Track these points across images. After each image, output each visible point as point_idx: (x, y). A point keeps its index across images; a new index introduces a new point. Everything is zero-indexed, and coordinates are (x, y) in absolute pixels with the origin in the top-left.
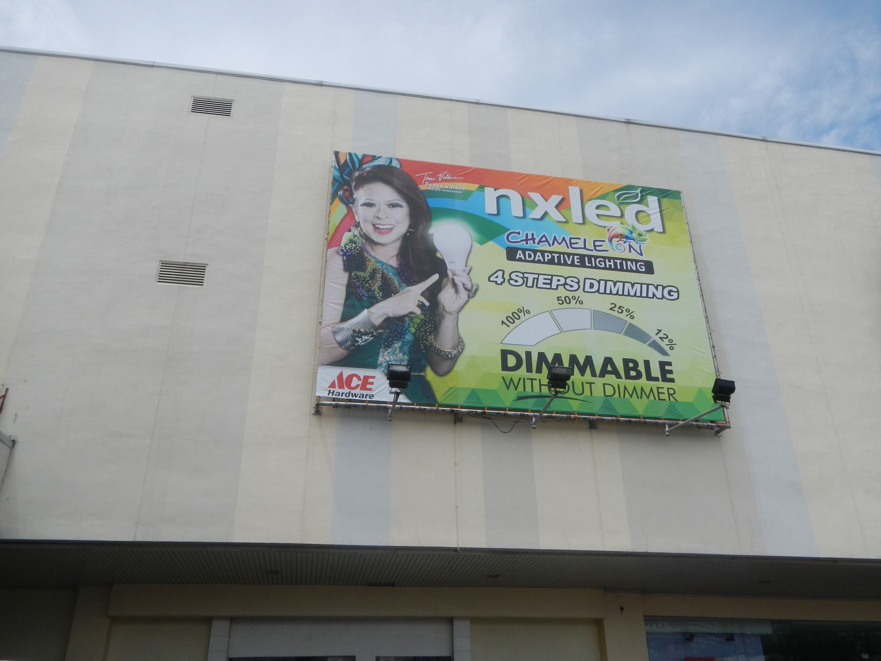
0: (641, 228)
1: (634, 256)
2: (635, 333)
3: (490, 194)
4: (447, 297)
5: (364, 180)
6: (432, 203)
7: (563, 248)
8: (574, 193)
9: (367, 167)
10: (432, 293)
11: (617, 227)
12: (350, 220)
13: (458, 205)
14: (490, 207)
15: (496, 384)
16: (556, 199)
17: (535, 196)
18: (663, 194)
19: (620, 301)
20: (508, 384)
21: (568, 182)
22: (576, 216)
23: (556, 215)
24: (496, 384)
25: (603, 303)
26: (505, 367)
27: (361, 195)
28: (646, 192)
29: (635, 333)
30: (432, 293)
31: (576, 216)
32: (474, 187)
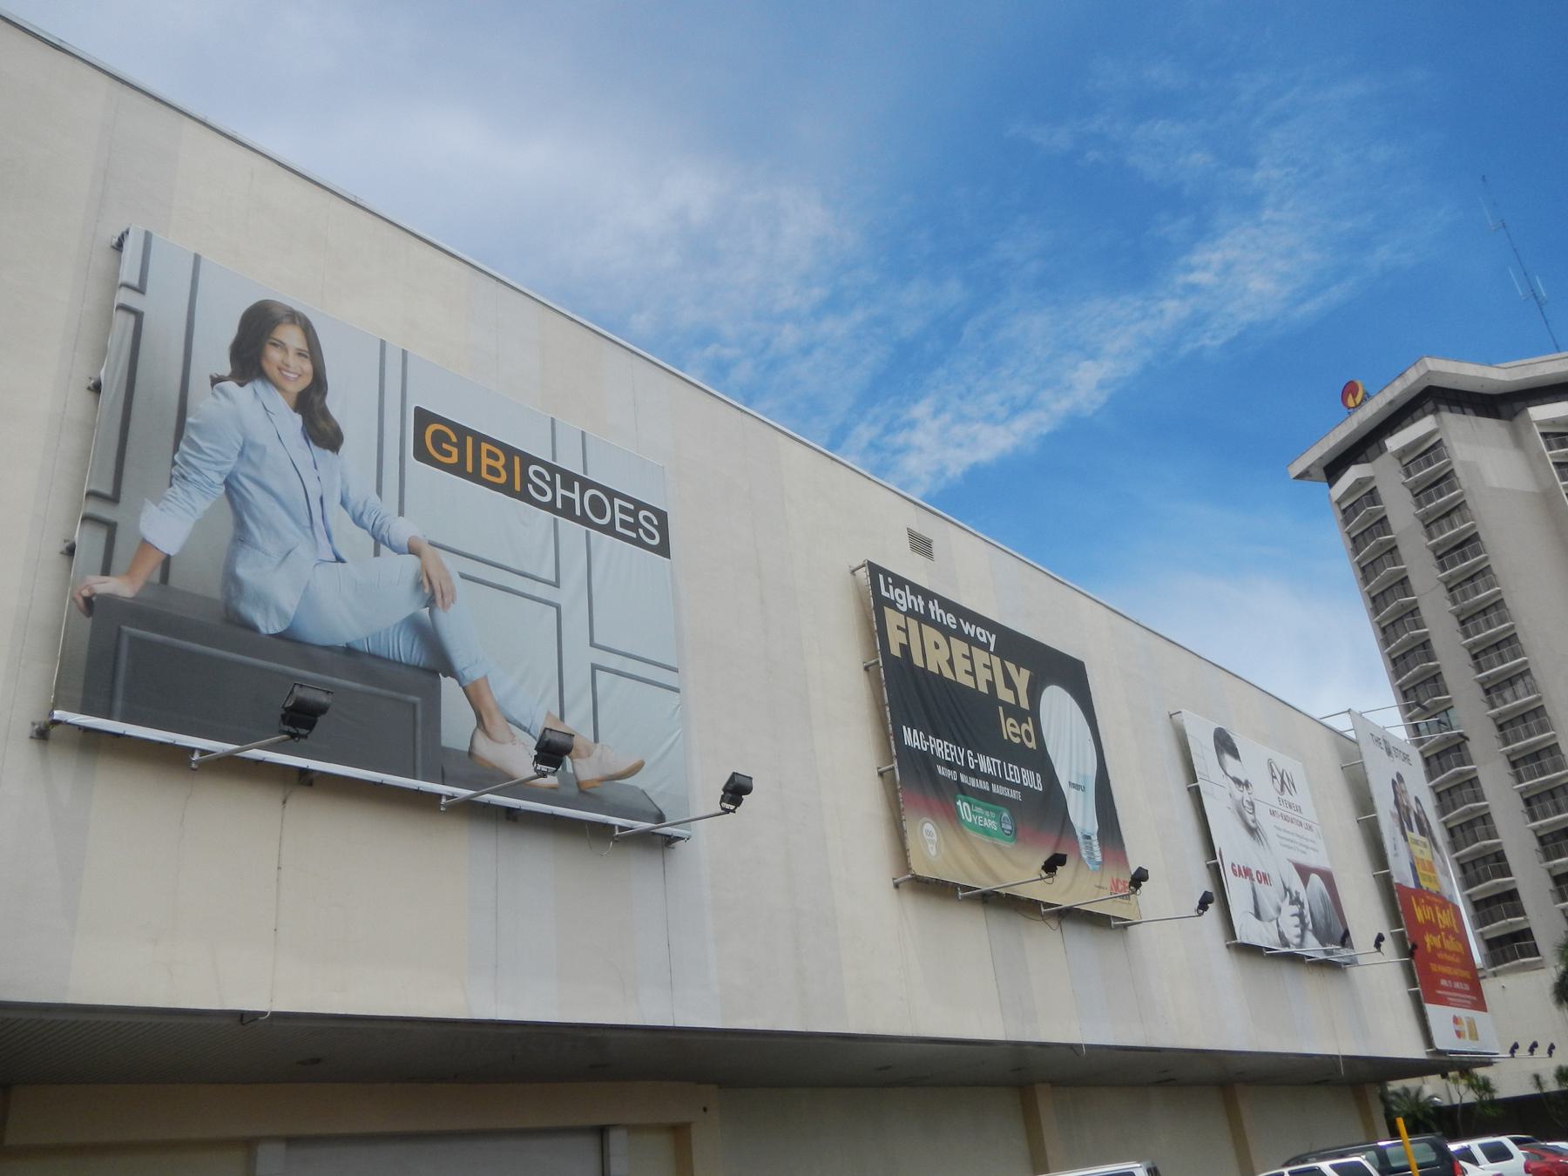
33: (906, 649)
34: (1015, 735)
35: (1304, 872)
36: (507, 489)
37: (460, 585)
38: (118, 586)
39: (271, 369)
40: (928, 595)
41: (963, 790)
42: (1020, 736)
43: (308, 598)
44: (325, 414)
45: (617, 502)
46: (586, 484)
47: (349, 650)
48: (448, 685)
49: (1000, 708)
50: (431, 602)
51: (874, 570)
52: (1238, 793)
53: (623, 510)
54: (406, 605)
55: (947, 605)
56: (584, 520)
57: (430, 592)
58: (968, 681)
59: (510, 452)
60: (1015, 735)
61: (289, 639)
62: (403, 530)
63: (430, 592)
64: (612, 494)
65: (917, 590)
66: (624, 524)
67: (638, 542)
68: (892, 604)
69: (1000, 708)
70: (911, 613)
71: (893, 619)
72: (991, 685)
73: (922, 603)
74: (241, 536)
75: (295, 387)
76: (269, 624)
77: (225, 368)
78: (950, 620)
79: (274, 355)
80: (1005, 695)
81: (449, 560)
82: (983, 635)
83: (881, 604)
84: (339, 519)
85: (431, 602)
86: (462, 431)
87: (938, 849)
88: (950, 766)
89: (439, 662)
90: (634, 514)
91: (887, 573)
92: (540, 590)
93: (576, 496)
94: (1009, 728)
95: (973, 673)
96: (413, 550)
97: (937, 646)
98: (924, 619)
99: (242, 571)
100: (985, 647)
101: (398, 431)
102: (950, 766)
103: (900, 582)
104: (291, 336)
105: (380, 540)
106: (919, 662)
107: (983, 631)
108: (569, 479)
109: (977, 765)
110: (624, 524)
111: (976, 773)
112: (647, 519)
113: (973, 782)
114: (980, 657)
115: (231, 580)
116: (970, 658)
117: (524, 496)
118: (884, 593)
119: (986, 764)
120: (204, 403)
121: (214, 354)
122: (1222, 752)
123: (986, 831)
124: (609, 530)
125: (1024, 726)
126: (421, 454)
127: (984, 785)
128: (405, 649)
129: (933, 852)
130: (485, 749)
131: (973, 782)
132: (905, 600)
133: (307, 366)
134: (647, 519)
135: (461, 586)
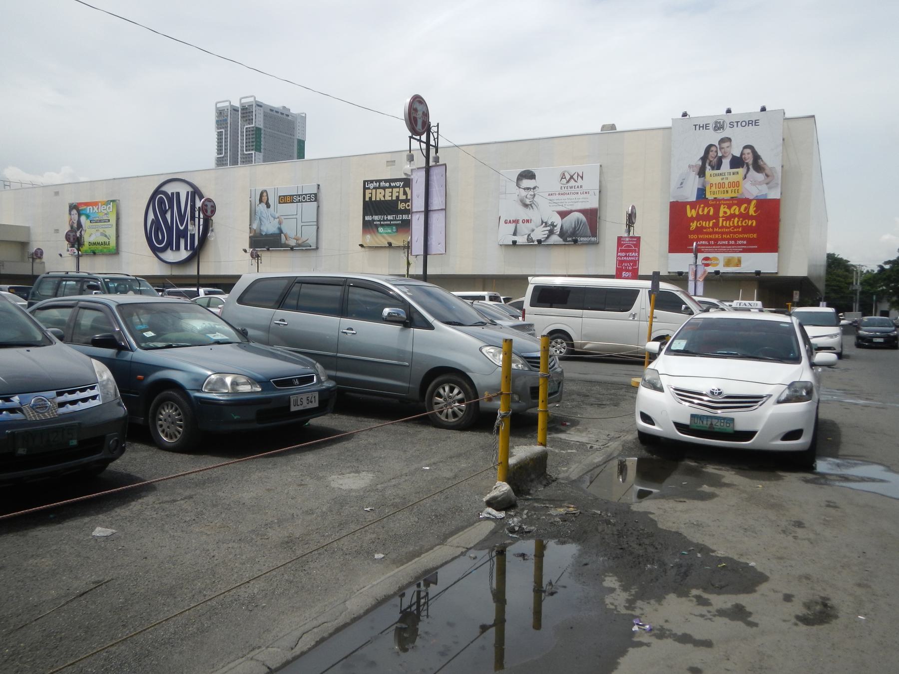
0: (109, 211)
1: (107, 218)
2: (106, 236)
3: (88, 208)
4: (83, 232)
5: (72, 209)
6: (81, 212)
7: (98, 219)
8: (100, 204)
9: (73, 206)
10: (81, 232)
11: (105, 212)
12: (71, 219)
13: (84, 212)
14: (88, 212)
15: (88, 249)
16: (97, 207)
17: (94, 207)
18: (113, 201)
19: (104, 229)
20: (90, 248)
21: (100, 202)
22: (100, 211)
23: (97, 211)
24: (88, 249)
25: (101, 230)
26: (89, 245)
27: (72, 213)
28: (111, 201)
29: (106, 236)
30: (81, 232)
31: (100, 211)
32: (85, 207)
33: (370, 198)
34: (403, 207)
35: (563, 214)
36: (291, 202)
37: (284, 220)
38: (252, 235)
39: (263, 200)
40: (380, 181)
41: (382, 225)
42: (405, 207)
43: (267, 230)
44: (269, 203)
45: (307, 195)
46: (302, 195)
47: (272, 234)
48: (282, 234)
49: (399, 202)
50: (280, 224)
51: (365, 182)
52: (524, 193)
53: (308, 197)
54: (277, 225)
55: (386, 181)
56: (302, 202)
57: (280, 223)
58: (390, 198)
59: (290, 196)
60: (403, 207)
61: (266, 235)
62: (277, 215)
63: (280, 223)
64: (306, 195)
65: (376, 181)
66: (308, 199)
67: (311, 201)
68: (369, 188)
69: (399, 202)
70: (374, 188)
71: (367, 192)
72: (398, 197)
73: (378, 184)
74: (261, 224)
75: (265, 202)
76: (264, 234)
77: (259, 203)
78: (387, 185)
79: (263, 198)
80: (402, 197)
81: (283, 217)
82: (398, 184)
83: (365, 189)
84: (270, 217)
85: (280, 224)
86: (284, 196)
87: (370, 240)
88: (378, 221)
89: (281, 231)
90: (310, 196)
91: (367, 181)
92: (294, 217)
93: (300, 198)
94: (401, 206)
95: (392, 196)
96: (278, 218)
97: (380, 193)
98: (379, 187)
99: (261, 228)
100: (399, 187)
101: (277, 200)
102: (378, 221)
103: (372, 182)
104: (265, 194)
105: (274, 218)
106: (373, 199)
107: (399, 183)
108: (299, 196)
109: (387, 219)
110: (308, 199)
111: (387, 220)
112: (313, 196)
113: (385, 223)
114: (395, 190)
115: (261, 230)
116: (392, 192)
117: (293, 202)
118: (367, 186)
119: (390, 217)
120: (257, 209)
121: (258, 202)
122: (522, 179)
123: (389, 233)
124: (306, 201)
125: (408, 203)
126: (280, 203)
127: (389, 223)
128: (277, 231)
129: (368, 241)
130: (287, 242)
131: (385, 223)
132: (371, 186)
133: (266, 197)
134: (313, 196)
135: (284, 220)
